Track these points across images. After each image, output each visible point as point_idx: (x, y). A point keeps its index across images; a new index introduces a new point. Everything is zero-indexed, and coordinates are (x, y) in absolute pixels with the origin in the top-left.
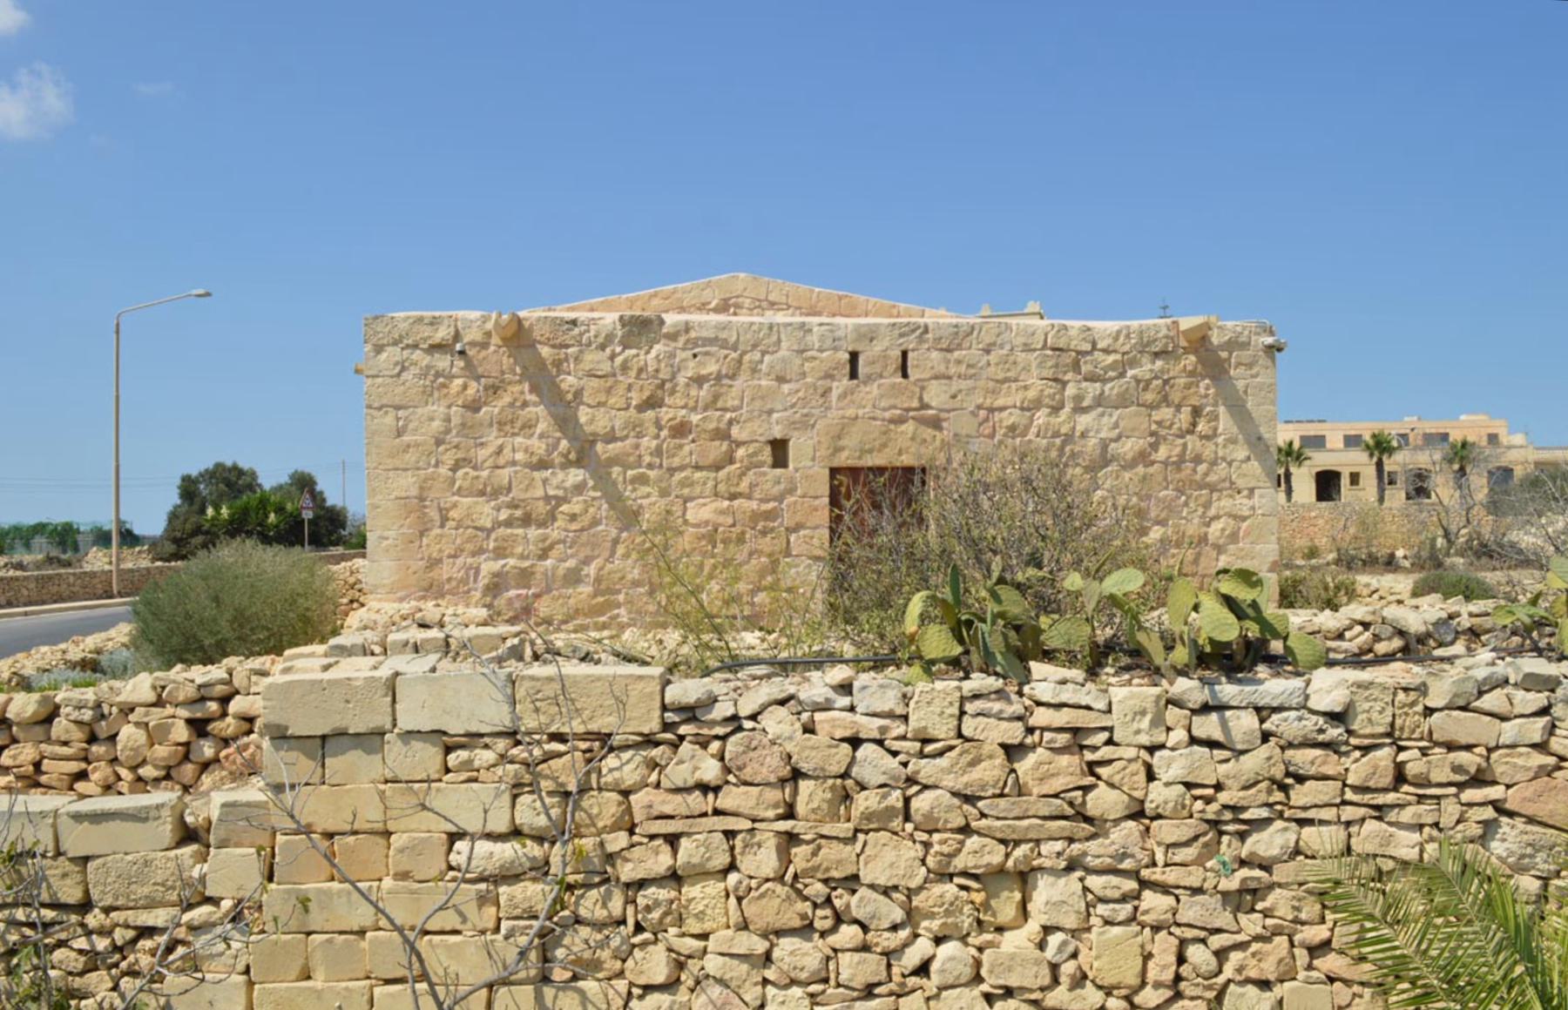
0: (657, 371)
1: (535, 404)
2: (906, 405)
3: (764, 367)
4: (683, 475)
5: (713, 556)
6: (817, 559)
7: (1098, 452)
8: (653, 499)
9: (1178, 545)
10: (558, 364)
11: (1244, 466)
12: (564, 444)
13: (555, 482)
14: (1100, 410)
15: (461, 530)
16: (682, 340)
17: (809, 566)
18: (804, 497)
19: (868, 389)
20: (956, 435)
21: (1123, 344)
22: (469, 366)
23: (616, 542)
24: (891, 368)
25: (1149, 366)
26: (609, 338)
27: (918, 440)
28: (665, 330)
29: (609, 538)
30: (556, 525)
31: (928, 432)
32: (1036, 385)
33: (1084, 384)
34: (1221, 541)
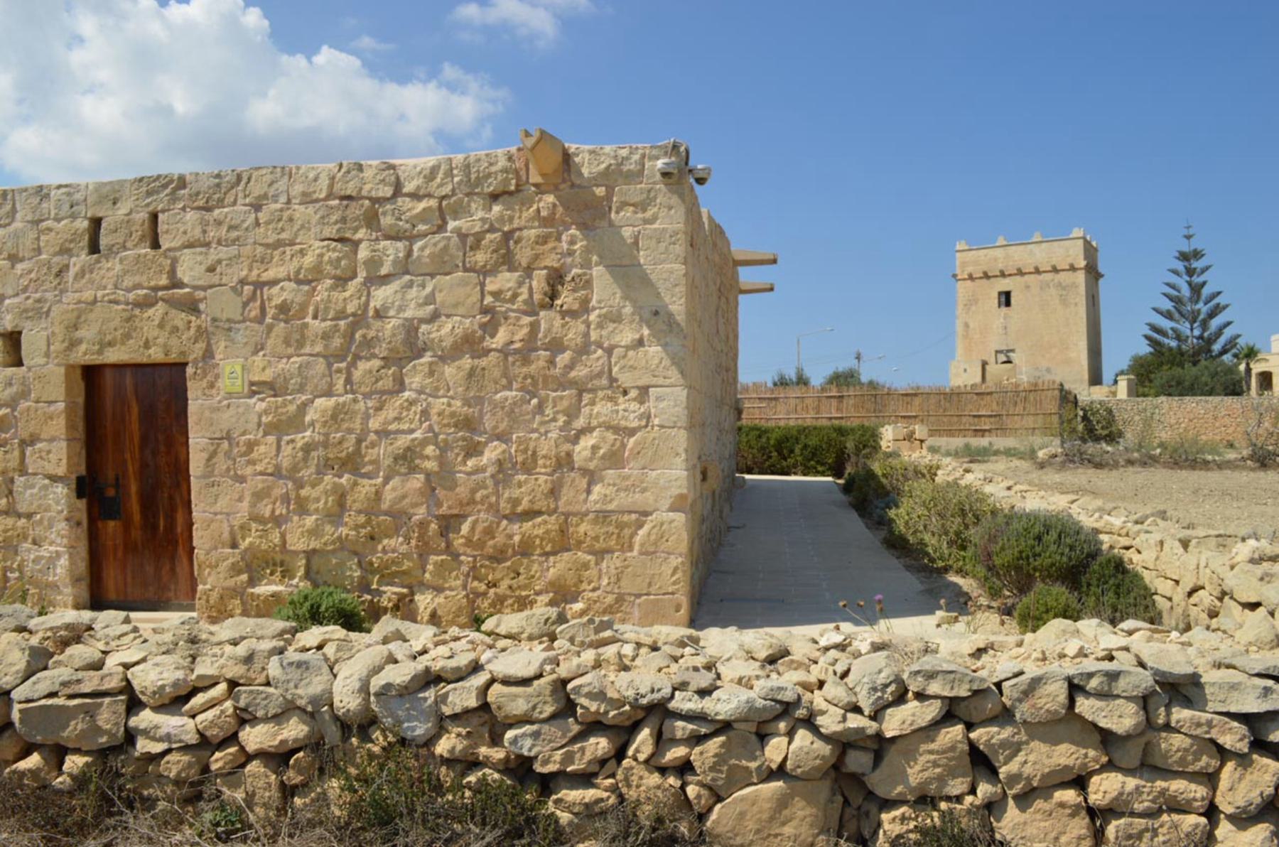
2: (153, 283)
6: (54, 479)
7: (400, 337)
9: (528, 467)
11: (631, 353)
14: (408, 277)
17: (45, 487)
18: (37, 402)
19: (109, 265)
20: (214, 320)
21: (441, 185)
24: (136, 236)
25: (480, 214)
27: (168, 328)
31: (179, 318)
32: (315, 250)
33: (383, 243)
34: (592, 466)
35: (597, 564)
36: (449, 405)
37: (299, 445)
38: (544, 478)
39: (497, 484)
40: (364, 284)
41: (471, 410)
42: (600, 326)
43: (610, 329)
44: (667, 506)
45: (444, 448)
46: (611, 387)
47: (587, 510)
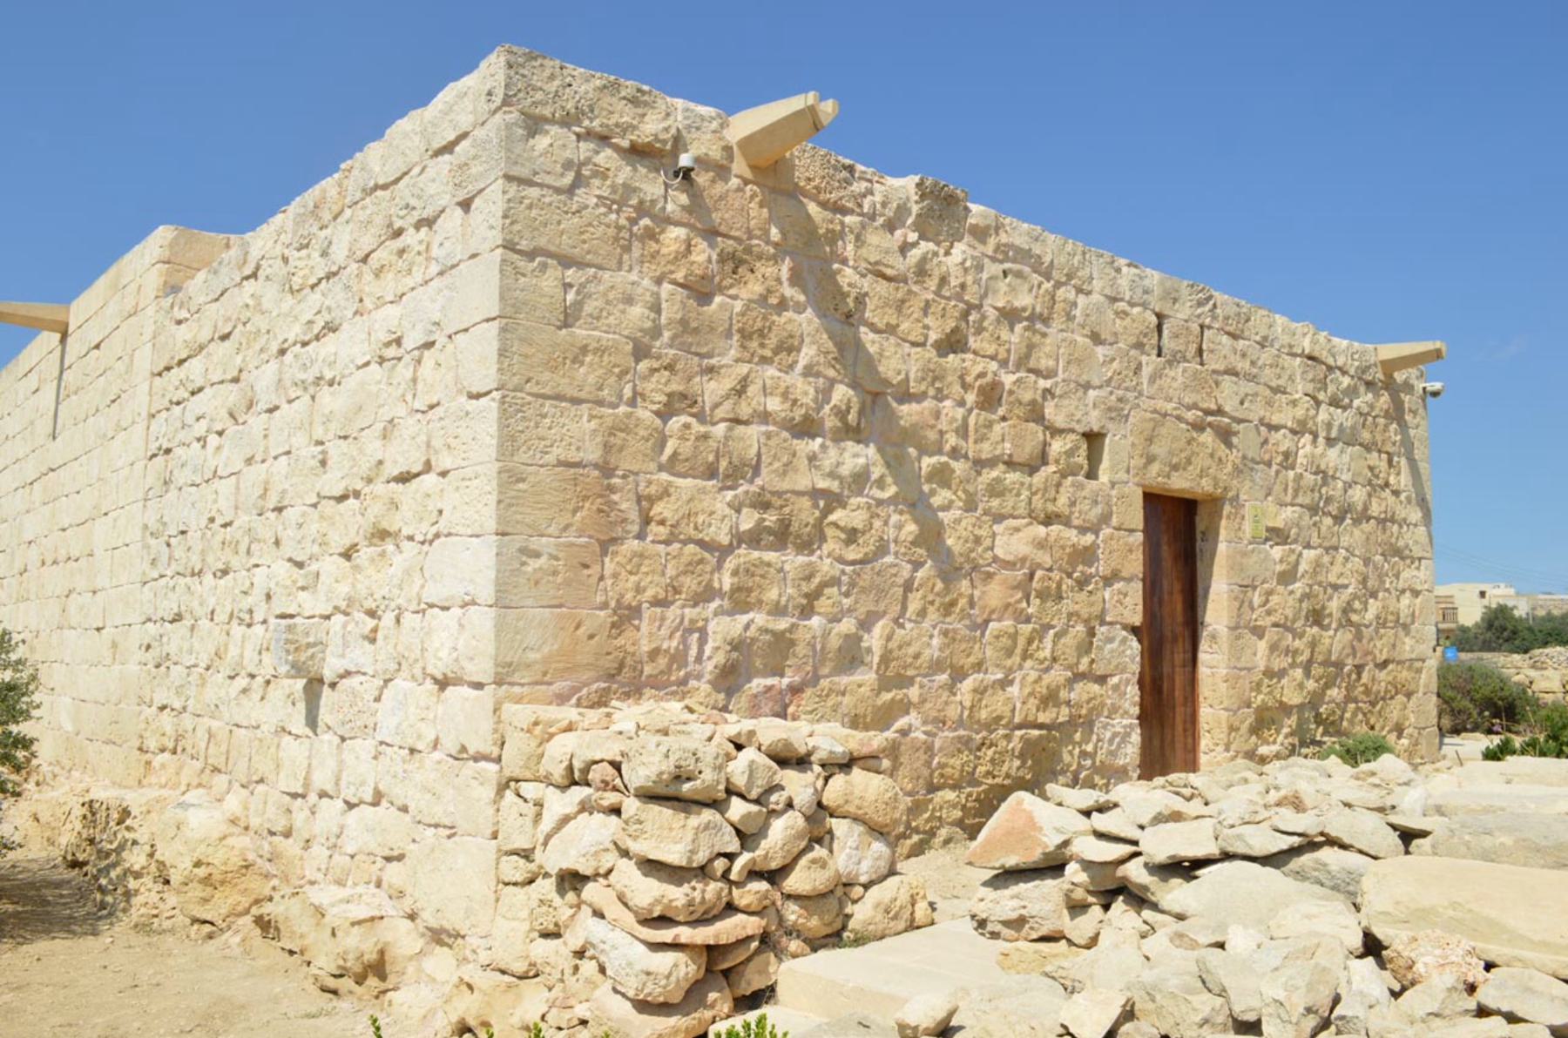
0: (963, 286)
1: (799, 309)
2: (1205, 405)
3: (1077, 312)
4: (995, 474)
5: (1028, 620)
8: (955, 513)
10: (834, 237)
12: (841, 393)
13: (827, 463)
15: (676, 546)
16: (992, 241)
17: (1124, 641)
20: (1244, 457)
22: (697, 205)
23: (908, 587)
26: (902, 210)
28: (971, 221)
29: (900, 581)
30: (826, 548)
31: (1222, 450)
37: (1298, 595)
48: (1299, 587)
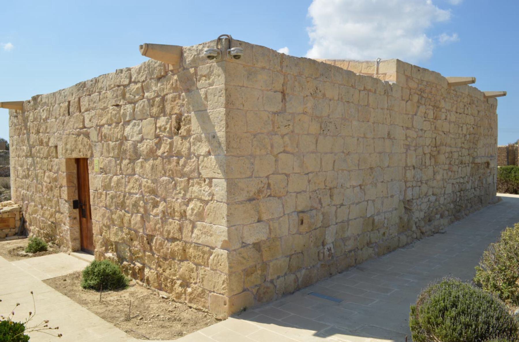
11: (206, 159)
14: (134, 121)
21: (142, 76)
34: (192, 218)
35: (197, 270)
36: (147, 182)
38: (177, 222)
39: (162, 223)
40: (123, 125)
41: (154, 185)
42: (194, 144)
43: (198, 145)
44: (220, 246)
45: (146, 203)
46: (199, 177)
47: (192, 241)
48: (111, 192)
